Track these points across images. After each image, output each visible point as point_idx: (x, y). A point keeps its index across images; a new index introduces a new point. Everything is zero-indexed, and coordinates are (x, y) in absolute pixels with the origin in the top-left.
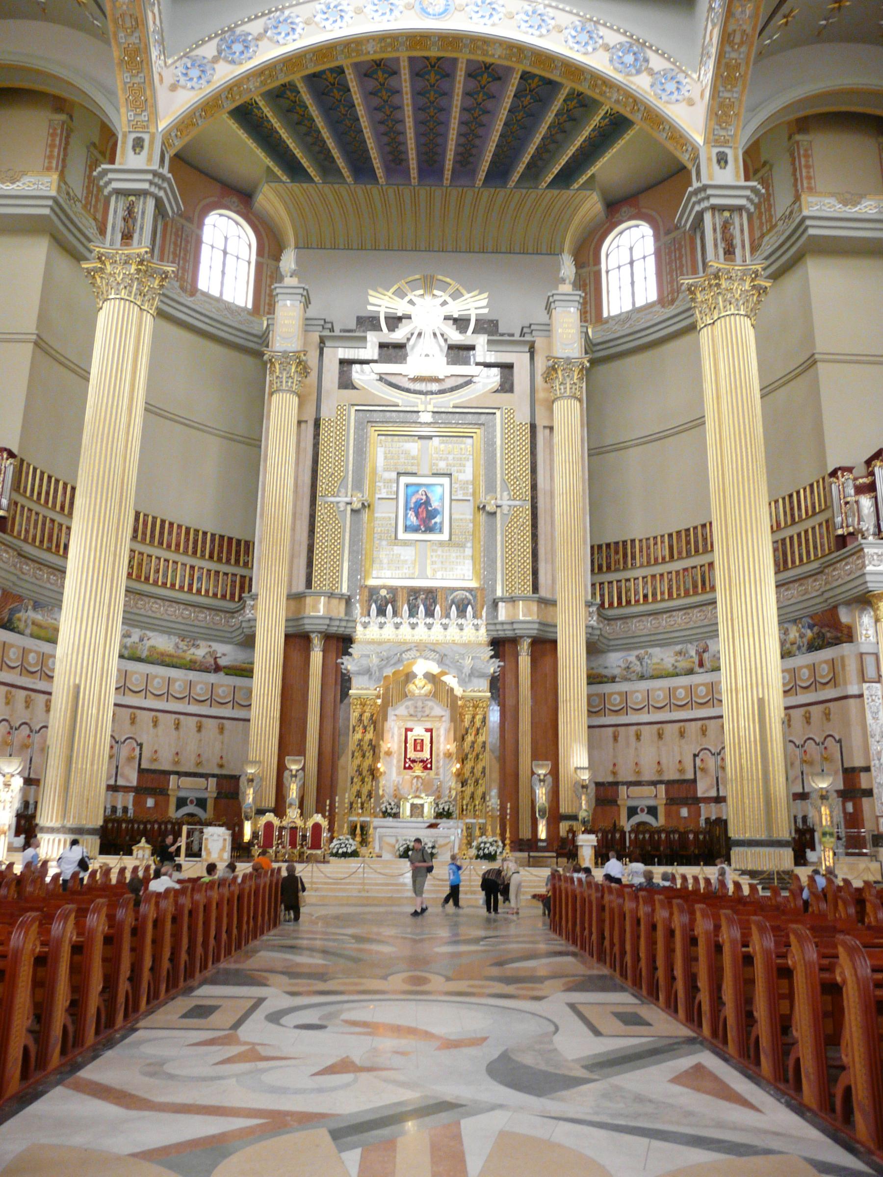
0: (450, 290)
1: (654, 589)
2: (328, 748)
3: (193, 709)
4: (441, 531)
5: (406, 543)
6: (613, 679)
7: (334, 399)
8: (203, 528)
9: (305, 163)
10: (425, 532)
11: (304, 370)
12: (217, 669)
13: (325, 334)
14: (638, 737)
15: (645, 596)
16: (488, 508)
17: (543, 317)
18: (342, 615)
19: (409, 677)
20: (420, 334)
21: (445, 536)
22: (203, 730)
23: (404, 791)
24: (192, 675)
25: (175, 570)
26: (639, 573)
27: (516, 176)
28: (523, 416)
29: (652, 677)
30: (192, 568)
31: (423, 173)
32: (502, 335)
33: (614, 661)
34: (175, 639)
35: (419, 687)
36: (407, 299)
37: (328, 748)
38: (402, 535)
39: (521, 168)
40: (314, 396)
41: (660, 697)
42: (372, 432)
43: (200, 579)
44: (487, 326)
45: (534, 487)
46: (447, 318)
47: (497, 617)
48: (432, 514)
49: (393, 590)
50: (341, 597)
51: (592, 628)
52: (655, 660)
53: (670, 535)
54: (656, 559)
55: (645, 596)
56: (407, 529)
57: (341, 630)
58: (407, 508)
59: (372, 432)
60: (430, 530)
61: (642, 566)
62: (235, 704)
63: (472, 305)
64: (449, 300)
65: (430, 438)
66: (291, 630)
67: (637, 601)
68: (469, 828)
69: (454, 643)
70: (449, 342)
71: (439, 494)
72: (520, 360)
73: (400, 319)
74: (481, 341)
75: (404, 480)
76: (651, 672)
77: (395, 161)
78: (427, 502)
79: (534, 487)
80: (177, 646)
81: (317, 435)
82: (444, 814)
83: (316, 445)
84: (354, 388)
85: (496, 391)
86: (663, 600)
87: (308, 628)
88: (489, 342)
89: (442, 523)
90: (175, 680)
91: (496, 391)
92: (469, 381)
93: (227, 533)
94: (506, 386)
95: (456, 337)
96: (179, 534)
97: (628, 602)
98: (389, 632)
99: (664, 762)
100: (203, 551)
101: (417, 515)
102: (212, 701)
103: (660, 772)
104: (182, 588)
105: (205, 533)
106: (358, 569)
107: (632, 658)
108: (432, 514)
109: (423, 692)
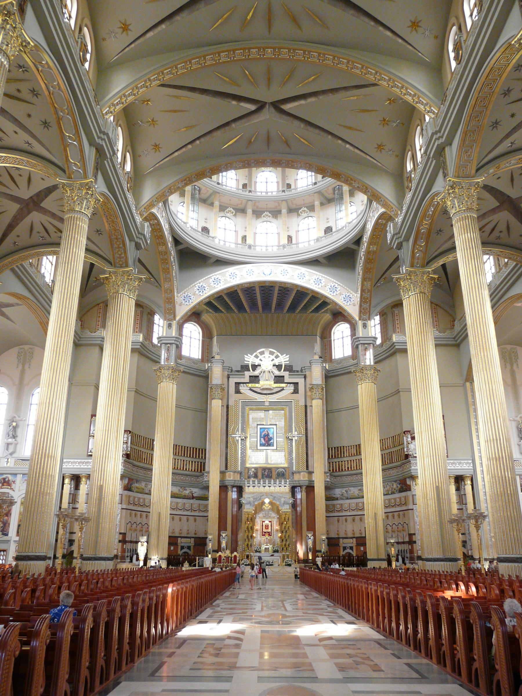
0: (275, 355)
1: (351, 465)
2: (235, 527)
3: (185, 513)
4: (273, 446)
5: (260, 450)
6: (337, 499)
7: (233, 397)
8: (187, 445)
9: (221, 308)
10: (267, 446)
11: (223, 389)
12: (193, 498)
13: (229, 373)
14: (346, 520)
15: (348, 468)
16: (290, 438)
17: (309, 365)
18: (239, 479)
19: (263, 503)
20: (264, 372)
21: (275, 448)
22: (189, 521)
23: (262, 542)
24: (185, 501)
25: (178, 462)
26: (345, 459)
27: (298, 310)
28: (302, 403)
29: (351, 499)
30: (184, 461)
31: (263, 308)
32: (294, 371)
33: (338, 492)
34: (179, 488)
35: (267, 506)
36: (259, 358)
37: (235, 527)
38: (259, 448)
39: (300, 308)
40: (226, 396)
41: (353, 506)
42: (247, 408)
43: (186, 465)
44: (289, 368)
45: (306, 429)
46: (274, 365)
47: (293, 478)
48: (270, 439)
49: (256, 469)
50: (238, 472)
51: (328, 482)
52: (352, 492)
53: (356, 446)
54: (352, 454)
55: (348, 468)
56: (261, 445)
57: (238, 485)
58: (260, 437)
59: (247, 408)
60: (269, 445)
61: (347, 456)
62: (200, 510)
63: (283, 361)
64: (275, 359)
65: (269, 411)
66: (221, 485)
67: (345, 470)
68: (284, 556)
69: (278, 493)
70: (275, 375)
71: (273, 432)
72: (301, 381)
73: (257, 366)
74: (286, 374)
75: (259, 427)
76: (350, 497)
77: (253, 305)
78: (268, 435)
79: (306, 429)
80: (179, 490)
81: (227, 411)
82: (276, 551)
83: (227, 415)
84: (241, 393)
85: (293, 393)
86: (354, 470)
87: (227, 484)
88: (289, 375)
89: (273, 442)
90: (179, 503)
91: (293, 393)
92: (283, 389)
93: (195, 447)
94: (296, 391)
95: (277, 373)
96: (179, 449)
97: (342, 470)
98: (256, 489)
99: (355, 530)
100: (187, 454)
101: (264, 440)
102: (192, 510)
103: (354, 534)
104: (180, 469)
105: (188, 447)
106: (243, 462)
107: (344, 491)
108: (270, 439)
109: (268, 508)
